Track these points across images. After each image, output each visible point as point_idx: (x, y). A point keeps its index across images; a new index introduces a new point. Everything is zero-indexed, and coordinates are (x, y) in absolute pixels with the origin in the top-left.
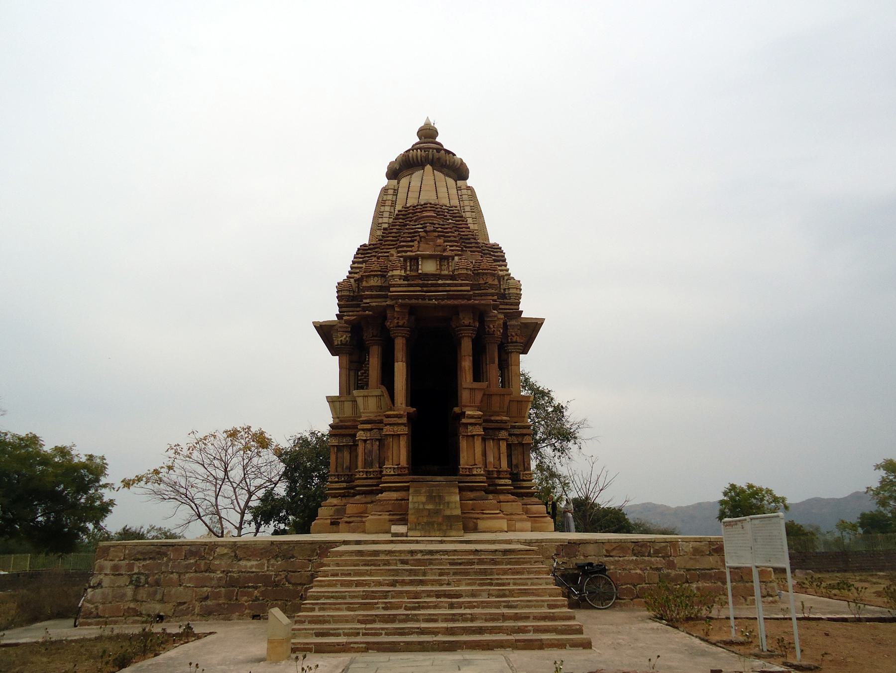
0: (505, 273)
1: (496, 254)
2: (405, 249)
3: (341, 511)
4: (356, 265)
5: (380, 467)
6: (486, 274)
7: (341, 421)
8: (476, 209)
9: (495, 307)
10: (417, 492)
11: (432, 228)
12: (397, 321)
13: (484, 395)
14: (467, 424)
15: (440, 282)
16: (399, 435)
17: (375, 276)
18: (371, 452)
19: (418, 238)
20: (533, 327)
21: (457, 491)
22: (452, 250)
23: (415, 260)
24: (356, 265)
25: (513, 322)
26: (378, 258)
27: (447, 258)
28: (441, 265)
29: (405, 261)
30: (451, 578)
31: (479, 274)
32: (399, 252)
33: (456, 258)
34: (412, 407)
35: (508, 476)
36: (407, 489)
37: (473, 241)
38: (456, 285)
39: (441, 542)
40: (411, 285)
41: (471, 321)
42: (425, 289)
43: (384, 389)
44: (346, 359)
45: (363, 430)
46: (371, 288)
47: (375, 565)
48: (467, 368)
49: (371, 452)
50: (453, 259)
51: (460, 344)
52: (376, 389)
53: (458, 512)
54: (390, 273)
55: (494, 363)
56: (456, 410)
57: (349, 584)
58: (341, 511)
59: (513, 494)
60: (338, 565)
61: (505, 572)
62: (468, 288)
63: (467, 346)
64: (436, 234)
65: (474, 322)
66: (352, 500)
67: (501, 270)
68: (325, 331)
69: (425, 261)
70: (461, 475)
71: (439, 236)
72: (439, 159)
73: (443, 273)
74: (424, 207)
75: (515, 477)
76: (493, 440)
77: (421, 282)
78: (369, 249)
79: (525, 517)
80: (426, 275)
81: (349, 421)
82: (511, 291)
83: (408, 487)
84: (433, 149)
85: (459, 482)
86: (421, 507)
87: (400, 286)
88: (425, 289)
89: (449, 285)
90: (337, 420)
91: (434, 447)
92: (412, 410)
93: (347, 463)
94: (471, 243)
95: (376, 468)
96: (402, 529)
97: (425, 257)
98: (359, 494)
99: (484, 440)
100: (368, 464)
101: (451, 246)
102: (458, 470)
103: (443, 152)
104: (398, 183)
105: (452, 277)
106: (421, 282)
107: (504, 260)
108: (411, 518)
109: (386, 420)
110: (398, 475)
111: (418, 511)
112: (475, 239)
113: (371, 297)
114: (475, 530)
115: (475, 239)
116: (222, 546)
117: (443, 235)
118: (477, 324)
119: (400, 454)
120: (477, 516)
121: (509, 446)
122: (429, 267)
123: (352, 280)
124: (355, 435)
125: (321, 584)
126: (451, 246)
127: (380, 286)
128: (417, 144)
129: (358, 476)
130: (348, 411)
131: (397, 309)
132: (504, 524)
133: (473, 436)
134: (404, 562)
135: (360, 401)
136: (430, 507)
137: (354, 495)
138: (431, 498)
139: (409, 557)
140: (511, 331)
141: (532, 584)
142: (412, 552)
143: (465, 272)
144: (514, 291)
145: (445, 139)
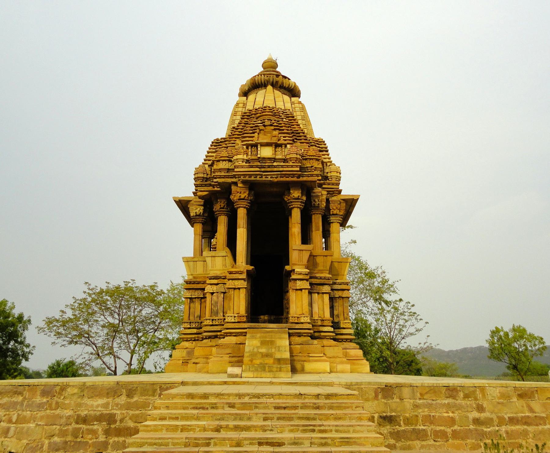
0: (327, 160)
1: (321, 146)
2: (247, 139)
3: (190, 353)
4: (210, 154)
5: (224, 316)
6: (312, 159)
7: (194, 277)
8: (305, 117)
9: (320, 186)
10: (253, 337)
11: (270, 124)
12: (239, 193)
13: (310, 256)
14: (296, 280)
15: (275, 164)
16: (239, 289)
17: (223, 160)
18: (216, 303)
19: (258, 131)
20: (350, 204)
21: (287, 336)
22: (285, 140)
23: (255, 146)
24: (210, 154)
25: (334, 198)
26: (227, 148)
27: (280, 145)
28: (275, 151)
29: (247, 148)
30: (275, 423)
31: (306, 159)
32: (242, 141)
33: (288, 146)
34: (251, 265)
35: (331, 324)
36: (245, 334)
37: (301, 134)
38: (288, 166)
39: (271, 383)
40: (252, 167)
41: (300, 195)
42: (263, 170)
43: (228, 250)
44: (199, 227)
45: (211, 284)
46: (220, 170)
47: (203, 408)
48: (296, 234)
49: (216, 303)
50: (286, 147)
51: (290, 214)
52: (223, 251)
53: (287, 355)
54: (235, 157)
55: (319, 230)
56: (287, 268)
57: (175, 428)
58: (190, 353)
59: (335, 340)
60: (168, 408)
61: (327, 417)
62: (298, 169)
63: (296, 216)
64: (273, 128)
65: (302, 196)
66: (199, 343)
67: (324, 158)
68: (183, 205)
69: (262, 148)
70: (292, 323)
71: (275, 129)
72: (277, 82)
73: (277, 157)
74: (264, 109)
75: (336, 325)
76: (318, 293)
77: (259, 164)
78: (221, 142)
79: (345, 360)
80: (264, 158)
81: (201, 277)
82: (333, 174)
83: (246, 333)
84: (274, 74)
85: (289, 329)
86: (255, 350)
87: (242, 167)
88: (263, 170)
89: (282, 166)
90: (191, 277)
91: (267, 299)
92: (251, 268)
93: (198, 313)
94: (301, 136)
95: (220, 316)
96: (236, 370)
97: (263, 145)
98: (206, 338)
99: (310, 293)
100: (214, 313)
101: (284, 137)
102: (287, 318)
103: (281, 77)
104: (247, 99)
105: (285, 160)
106: (259, 164)
107: (327, 151)
108: (246, 360)
109: (229, 276)
110: (238, 322)
111: (253, 355)
112: (304, 133)
113: (220, 177)
114: (303, 371)
115: (304, 133)
116: (73, 386)
117: (278, 128)
118: (304, 198)
119: (240, 303)
120: (304, 359)
121: (332, 299)
122: (266, 152)
123: (206, 166)
124: (204, 289)
125: (148, 429)
126: (284, 137)
127: (228, 169)
128: (262, 72)
129: (205, 323)
130: (200, 270)
131: (240, 185)
132: (326, 366)
133: (301, 290)
134: (232, 406)
135: (209, 260)
136: (263, 350)
137: (203, 339)
138: (263, 343)
139: (237, 401)
140: (332, 206)
141: (354, 431)
142: (240, 396)
143: (295, 156)
144: (335, 174)
145: (282, 69)
